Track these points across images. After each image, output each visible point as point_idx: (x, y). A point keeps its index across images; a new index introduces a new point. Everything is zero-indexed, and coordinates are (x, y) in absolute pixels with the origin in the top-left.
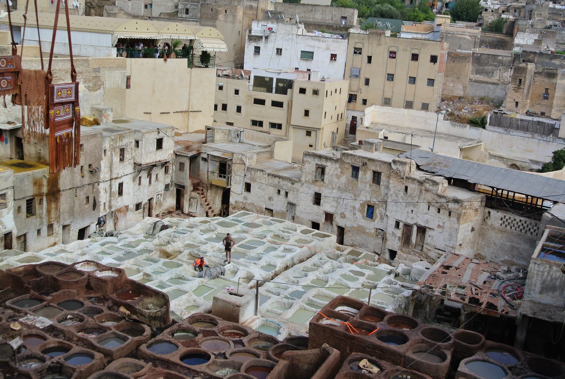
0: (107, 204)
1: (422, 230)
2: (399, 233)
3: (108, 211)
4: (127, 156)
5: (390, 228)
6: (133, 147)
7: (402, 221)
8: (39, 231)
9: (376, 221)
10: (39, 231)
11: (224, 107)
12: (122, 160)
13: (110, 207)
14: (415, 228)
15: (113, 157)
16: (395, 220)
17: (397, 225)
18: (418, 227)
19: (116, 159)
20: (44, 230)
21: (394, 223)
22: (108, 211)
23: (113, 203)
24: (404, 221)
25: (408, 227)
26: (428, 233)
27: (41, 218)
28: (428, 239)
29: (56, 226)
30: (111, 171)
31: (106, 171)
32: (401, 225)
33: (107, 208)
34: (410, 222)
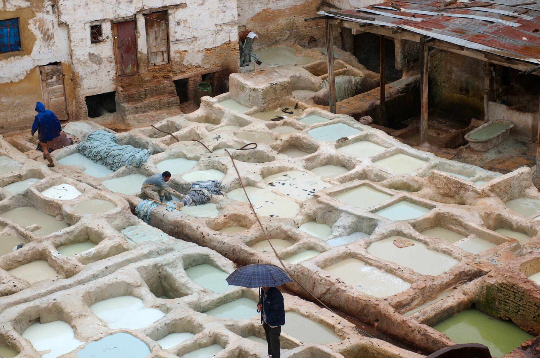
1: (158, 17)
2: (106, 49)
5: (84, 47)
7: (103, 21)
9: (35, 49)
14: (141, 22)
16: (88, 25)
17: (96, 33)
18: (144, 15)
21: (88, 33)
24: (112, 16)
25: (124, 27)
26: (174, 17)
28: (176, 31)
32: (107, 29)
34: (126, 11)
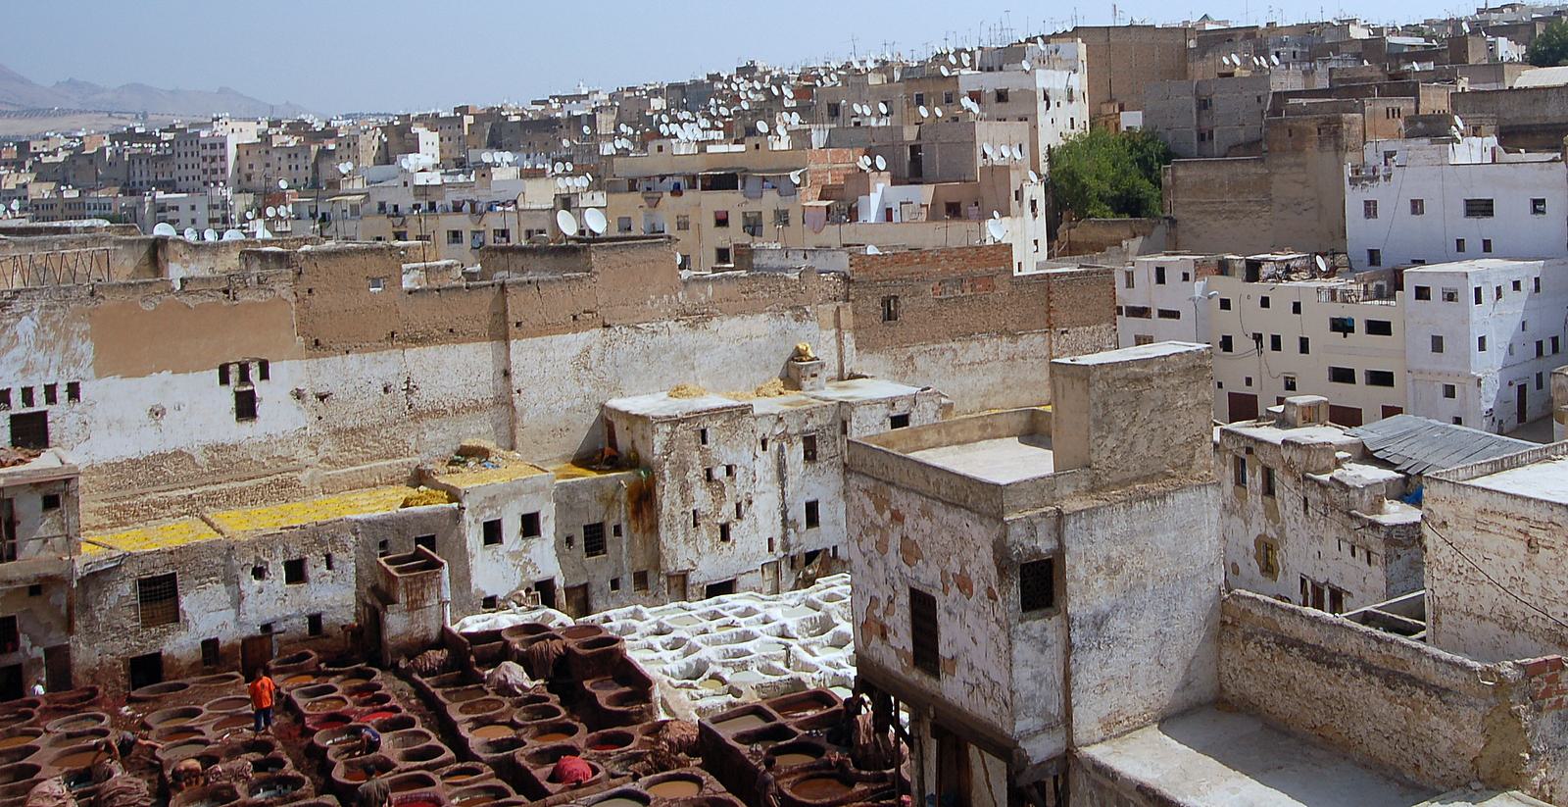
0: (778, 542)
3: (781, 554)
4: (822, 450)
6: (837, 435)
8: (615, 584)
10: (615, 584)
11: (1276, 343)
12: (810, 455)
13: (786, 547)
15: (786, 452)
19: (796, 453)
20: (627, 580)
22: (781, 554)
23: (793, 538)
27: (619, 561)
29: (651, 575)
30: (782, 478)
31: (768, 478)
33: (777, 547)
